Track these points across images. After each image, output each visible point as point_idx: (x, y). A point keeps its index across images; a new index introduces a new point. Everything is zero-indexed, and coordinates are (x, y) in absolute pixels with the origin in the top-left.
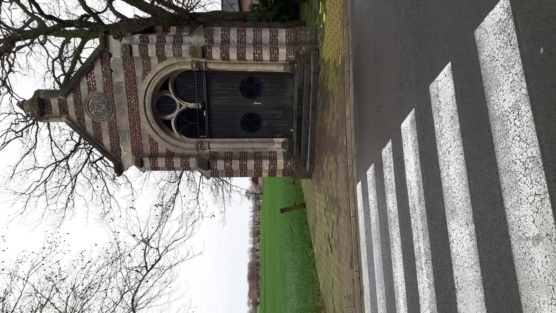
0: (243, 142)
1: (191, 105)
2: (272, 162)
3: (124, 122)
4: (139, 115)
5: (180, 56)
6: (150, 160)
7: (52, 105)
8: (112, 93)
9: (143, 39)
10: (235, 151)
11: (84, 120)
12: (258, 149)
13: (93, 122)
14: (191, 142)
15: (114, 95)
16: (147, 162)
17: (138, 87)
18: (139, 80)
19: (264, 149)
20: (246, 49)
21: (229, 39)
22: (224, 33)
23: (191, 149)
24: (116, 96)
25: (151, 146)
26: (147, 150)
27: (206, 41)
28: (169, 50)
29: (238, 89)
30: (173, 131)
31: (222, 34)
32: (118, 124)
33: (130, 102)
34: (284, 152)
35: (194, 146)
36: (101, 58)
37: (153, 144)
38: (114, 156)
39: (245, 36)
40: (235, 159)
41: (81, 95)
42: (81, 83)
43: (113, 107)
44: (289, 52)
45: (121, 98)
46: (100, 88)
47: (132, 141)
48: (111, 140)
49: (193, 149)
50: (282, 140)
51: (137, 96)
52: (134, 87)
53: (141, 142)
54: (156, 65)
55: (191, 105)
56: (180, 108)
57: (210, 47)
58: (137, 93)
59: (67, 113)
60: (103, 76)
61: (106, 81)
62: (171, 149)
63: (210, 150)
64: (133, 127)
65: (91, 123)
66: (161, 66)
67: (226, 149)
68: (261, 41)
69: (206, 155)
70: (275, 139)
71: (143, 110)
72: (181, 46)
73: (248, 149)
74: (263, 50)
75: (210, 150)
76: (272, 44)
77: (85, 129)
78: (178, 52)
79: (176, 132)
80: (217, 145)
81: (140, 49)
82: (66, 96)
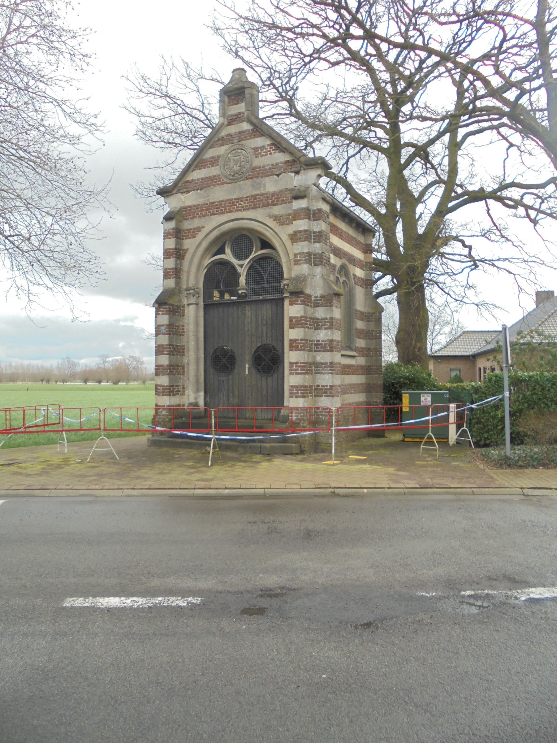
0: (197, 349)
1: (243, 280)
2: (166, 389)
3: (219, 194)
4: (227, 212)
5: (296, 263)
6: (173, 229)
7: (239, 105)
8: (252, 178)
9: (317, 213)
10: (185, 338)
11: (222, 145)
12: (188, 370)
13: (219, 157)
14: (197, 280)
15: (250, 180)
16: (172, 225)
17: (260, 210)
18: (268, 210)
19: (188, 379)
20: (302, 352)
21: (320, 329)
22: (328, 322)
23: (188, 280)
24: (249, 182)
25: (191, 229)
26: (187, 225)
27: (317, 297)
28: (303, 247)
29: (265, 342)
30: (213, 256)
31: (326, 319)
32: (217, 188)
33: (242, 201)
34: (183, 405)
35: (191, 283)
36: (294, 161)
37: (193, 232)
38: (180, 185)
39: (324, 351)
40: (170, 339)
41: (250, 139)
42: (263, 137)
43: (236, 179)
44: (300, 413)
45: (246, 189)
46: (258, 162)
47: (197, 207)
48: (198, 180)
49: (187, 283)
50: (201, 403)
51: (249, 209)
52: (259, 204)
53: (195, 217)
54: (285, 232)
55: (243, 280)
56: (239, 265)
57: (303, 303)
58: (253, 208)
59: (229, 124)
60: (272, 165)
61: (266, 169)
62: (188, 256)
63: (186, 306)
64: (213, 206)
65: (217, 154)
66: (285, 238)
67: (188, 326)
68: (319, 373)
69: (180, 301)
70: (202, 394)
71: (233, 218)
72: (307, 263)
73: (188, 357)
74: (301, 376)
75: (186, 306)
76: (315, 389)
77: (211, 147)
78: (300, 260)
79: (210, 261)
80: (193, 316)
81: (302, 209)
82: (249, 121)
